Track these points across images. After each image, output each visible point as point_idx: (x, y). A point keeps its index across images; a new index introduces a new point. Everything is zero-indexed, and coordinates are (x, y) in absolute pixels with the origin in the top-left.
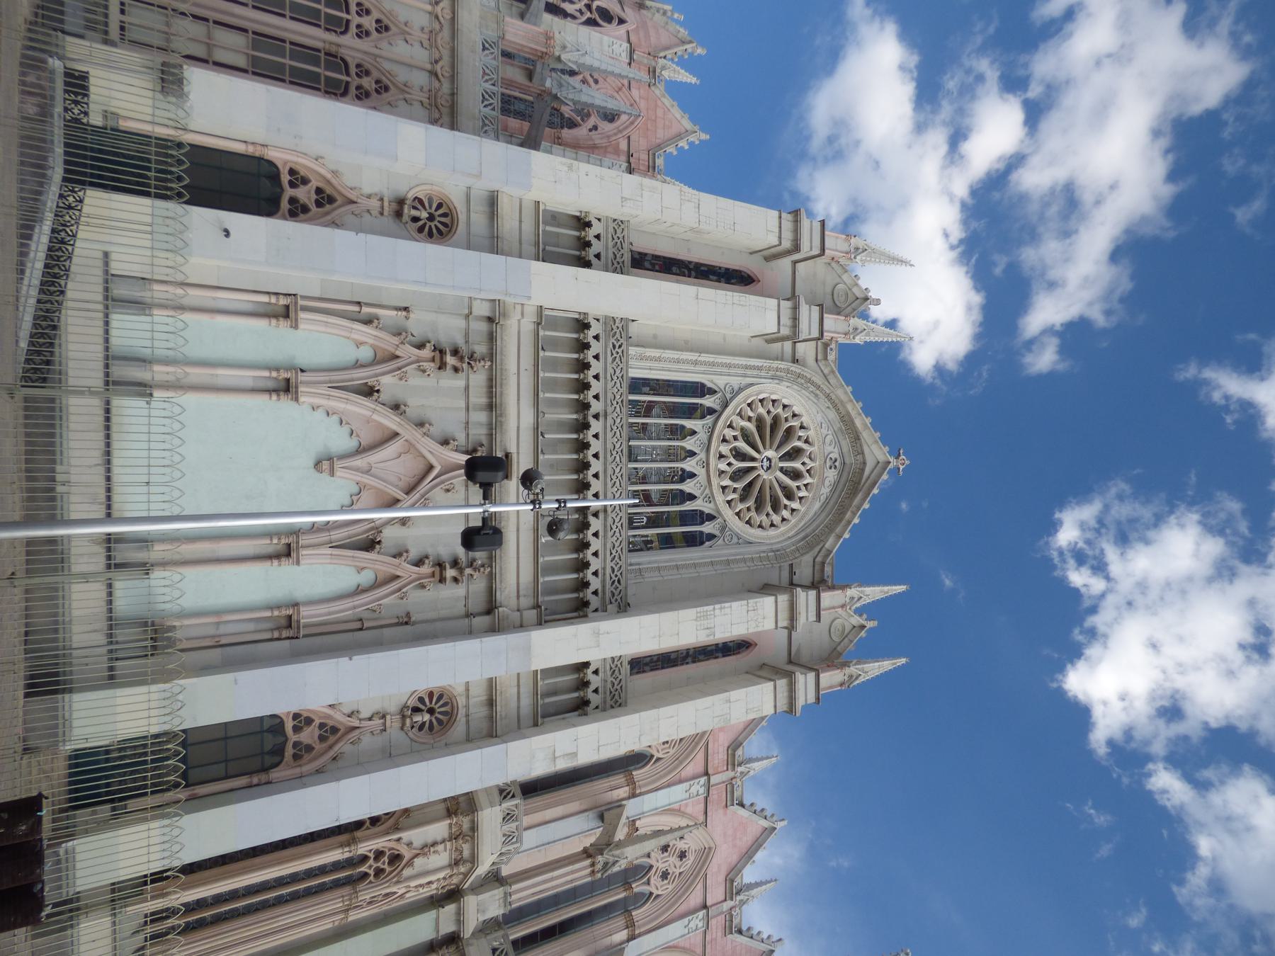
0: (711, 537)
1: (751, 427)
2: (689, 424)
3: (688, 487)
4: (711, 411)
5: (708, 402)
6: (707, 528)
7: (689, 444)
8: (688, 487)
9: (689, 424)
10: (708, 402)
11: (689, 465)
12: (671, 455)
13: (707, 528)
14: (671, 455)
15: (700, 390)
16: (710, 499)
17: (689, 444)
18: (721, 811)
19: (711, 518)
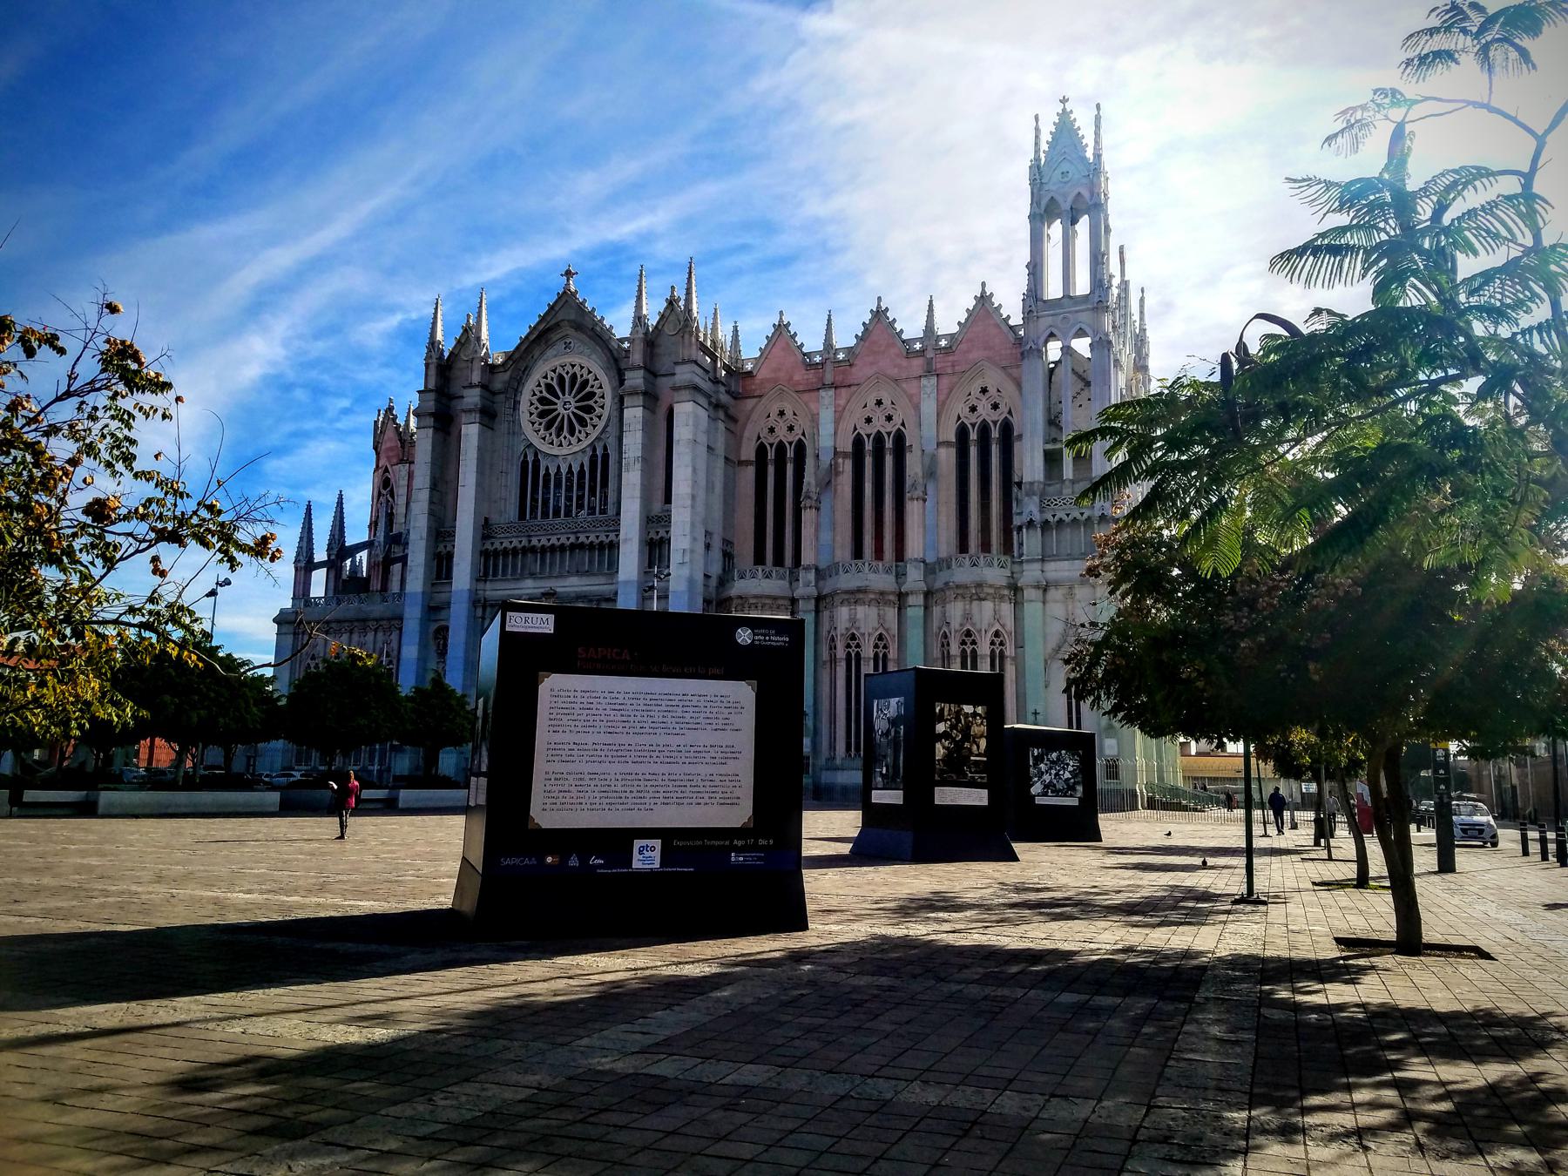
0: (605, 448)
1: (544, 421)
2: (542, 472)
3: (576, 469)
4: (536, 455)
5: (530, 458)
6: (599, 452)
7: (552, 471)
8: (576, 469)
9: (542, 472)
10: (530, 458)
11: (564, 470)
12: (558, 485)
13: (599, 452)
14: (558, 485)
15: (525, 463)
16: (583, 451)
17: (552, 471)
18: (854, 370)
19: (594, 450)
